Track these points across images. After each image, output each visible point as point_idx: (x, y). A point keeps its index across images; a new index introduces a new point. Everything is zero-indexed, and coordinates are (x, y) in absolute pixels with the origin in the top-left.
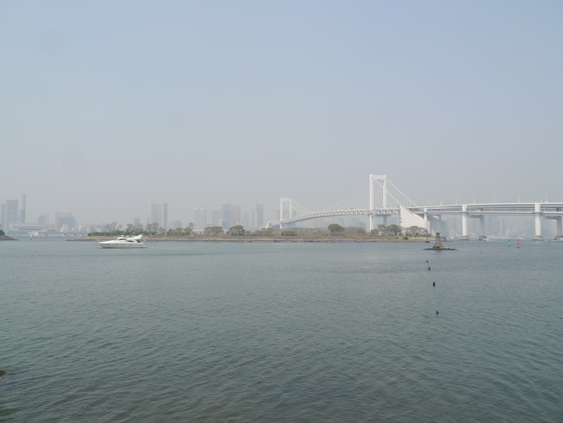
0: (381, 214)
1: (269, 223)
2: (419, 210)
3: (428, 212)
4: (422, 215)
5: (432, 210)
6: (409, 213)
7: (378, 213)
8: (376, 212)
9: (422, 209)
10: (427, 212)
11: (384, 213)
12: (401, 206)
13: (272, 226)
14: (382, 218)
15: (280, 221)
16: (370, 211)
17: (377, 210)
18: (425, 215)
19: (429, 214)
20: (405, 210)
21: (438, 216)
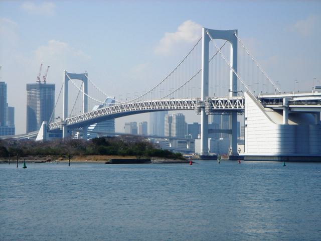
0: (219, 108)
1: (45, 125)
3: (290, 106)
4: (280, 112)
6: (257, 107)
8: (212, 105)
10: (287, 106)
11: (224, 108)
12: (246, 94)
17: (214, 101)
18: (284, 112)
20: (251, 101)
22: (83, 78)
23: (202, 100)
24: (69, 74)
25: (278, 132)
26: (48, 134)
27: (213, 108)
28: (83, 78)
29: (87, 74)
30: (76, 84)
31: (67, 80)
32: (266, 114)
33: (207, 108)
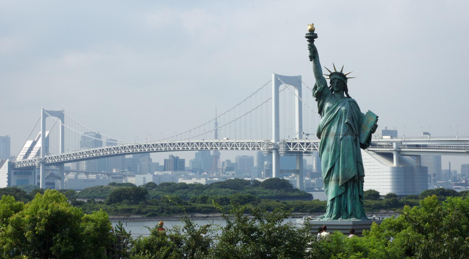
0: (298, 150)
1: (9, 163)
2: (381, 146)
4: (388, 156)
5: (408, 146)
7: (291, 149)
8: (287, 147)
9: (379, 144)
10: (399, 150)
11: (305, 149)
13: (15, 169)
14: (294, 158)
15: (41, 159)
16: (274, 144)
17: (289, 144)
19: (402, 153)
21: (415, 157)
22: (60, 115)
23: (273, 141)
24: (47, 111)
25: (389, 173)
26: (13, 172)
27: (289, 149)
28: (60, 115)
29: (64, 111)
30: (51, 120)
31: (45, 116)
32: (371, 155)
33: (282, 150)
